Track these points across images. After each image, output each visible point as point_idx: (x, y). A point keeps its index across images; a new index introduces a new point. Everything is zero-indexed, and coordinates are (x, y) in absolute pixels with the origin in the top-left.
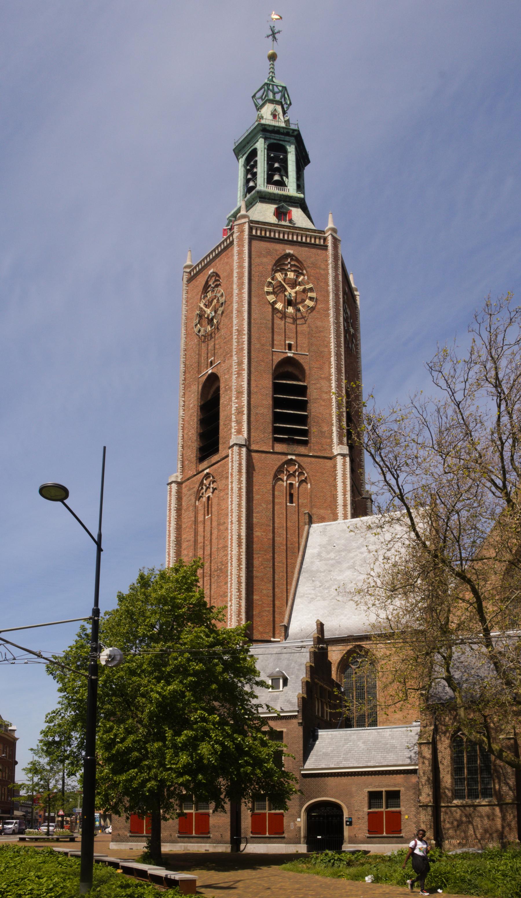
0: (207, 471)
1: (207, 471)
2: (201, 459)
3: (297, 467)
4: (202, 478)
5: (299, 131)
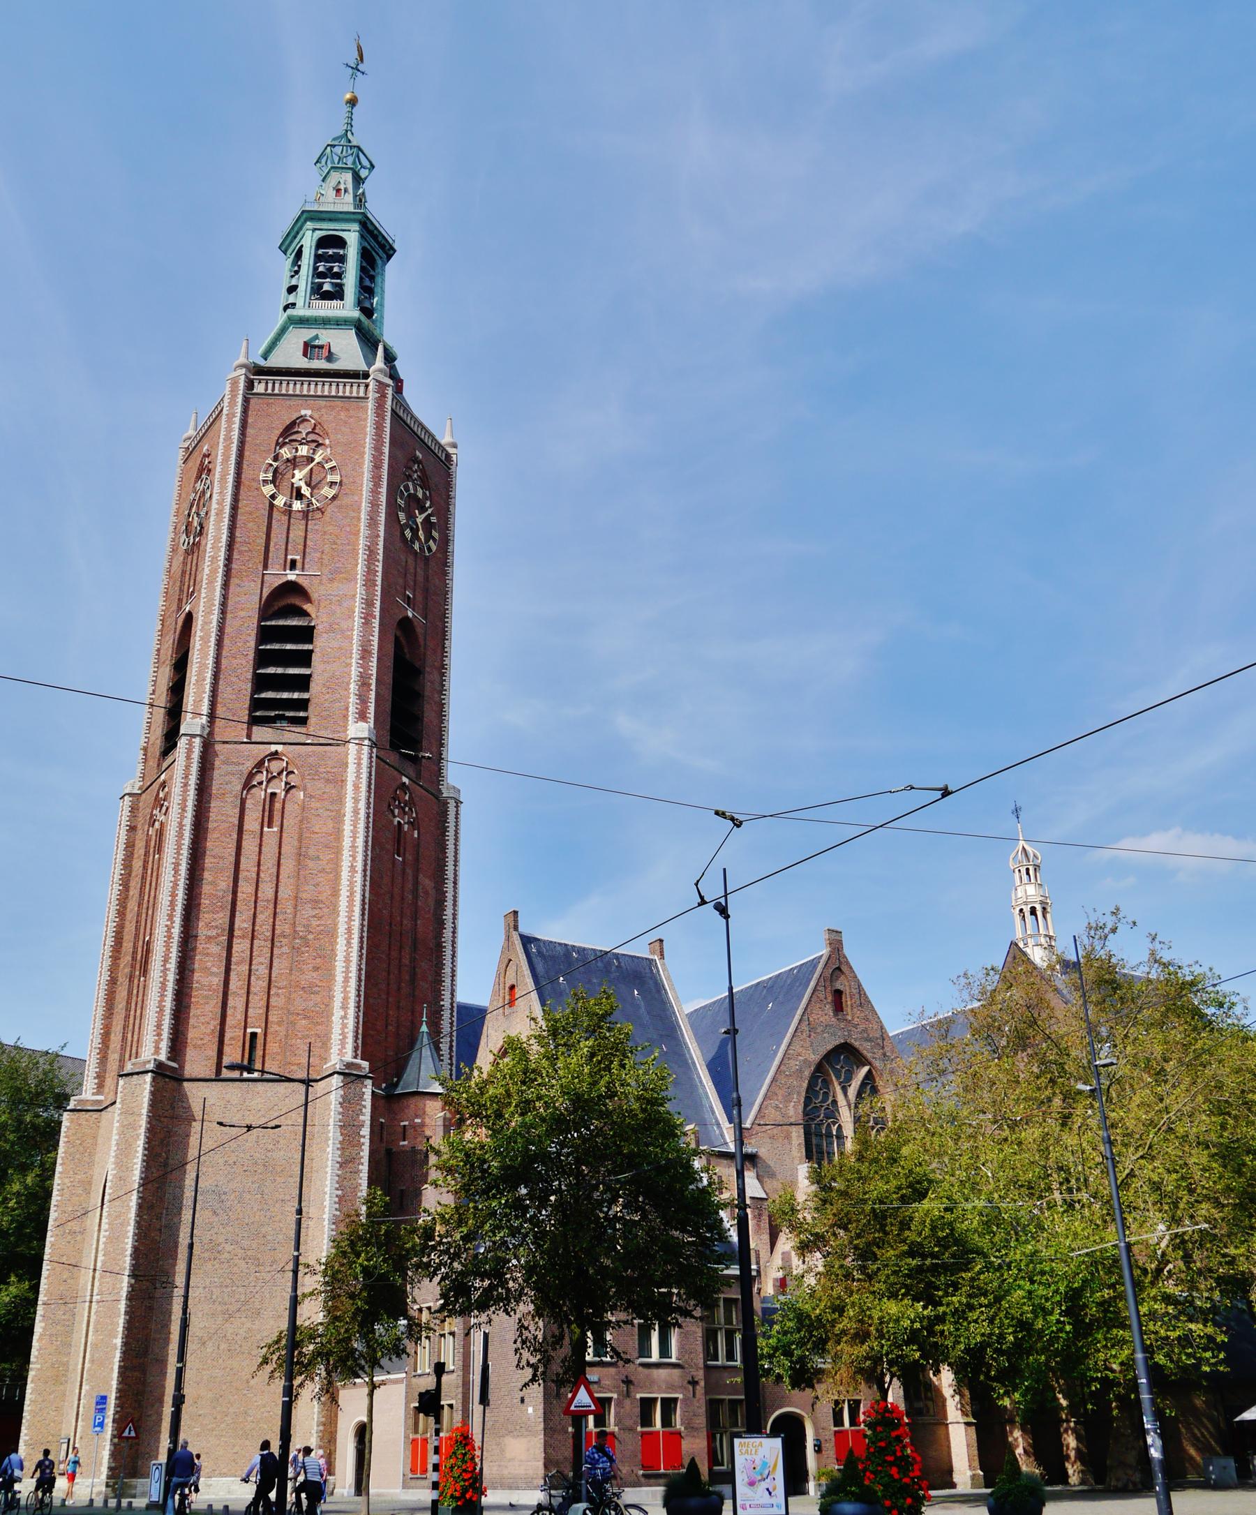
0: (280, 748)
1: (280, 748)
2: (254, 721)
3: (407, 798)
5: (395, 251)
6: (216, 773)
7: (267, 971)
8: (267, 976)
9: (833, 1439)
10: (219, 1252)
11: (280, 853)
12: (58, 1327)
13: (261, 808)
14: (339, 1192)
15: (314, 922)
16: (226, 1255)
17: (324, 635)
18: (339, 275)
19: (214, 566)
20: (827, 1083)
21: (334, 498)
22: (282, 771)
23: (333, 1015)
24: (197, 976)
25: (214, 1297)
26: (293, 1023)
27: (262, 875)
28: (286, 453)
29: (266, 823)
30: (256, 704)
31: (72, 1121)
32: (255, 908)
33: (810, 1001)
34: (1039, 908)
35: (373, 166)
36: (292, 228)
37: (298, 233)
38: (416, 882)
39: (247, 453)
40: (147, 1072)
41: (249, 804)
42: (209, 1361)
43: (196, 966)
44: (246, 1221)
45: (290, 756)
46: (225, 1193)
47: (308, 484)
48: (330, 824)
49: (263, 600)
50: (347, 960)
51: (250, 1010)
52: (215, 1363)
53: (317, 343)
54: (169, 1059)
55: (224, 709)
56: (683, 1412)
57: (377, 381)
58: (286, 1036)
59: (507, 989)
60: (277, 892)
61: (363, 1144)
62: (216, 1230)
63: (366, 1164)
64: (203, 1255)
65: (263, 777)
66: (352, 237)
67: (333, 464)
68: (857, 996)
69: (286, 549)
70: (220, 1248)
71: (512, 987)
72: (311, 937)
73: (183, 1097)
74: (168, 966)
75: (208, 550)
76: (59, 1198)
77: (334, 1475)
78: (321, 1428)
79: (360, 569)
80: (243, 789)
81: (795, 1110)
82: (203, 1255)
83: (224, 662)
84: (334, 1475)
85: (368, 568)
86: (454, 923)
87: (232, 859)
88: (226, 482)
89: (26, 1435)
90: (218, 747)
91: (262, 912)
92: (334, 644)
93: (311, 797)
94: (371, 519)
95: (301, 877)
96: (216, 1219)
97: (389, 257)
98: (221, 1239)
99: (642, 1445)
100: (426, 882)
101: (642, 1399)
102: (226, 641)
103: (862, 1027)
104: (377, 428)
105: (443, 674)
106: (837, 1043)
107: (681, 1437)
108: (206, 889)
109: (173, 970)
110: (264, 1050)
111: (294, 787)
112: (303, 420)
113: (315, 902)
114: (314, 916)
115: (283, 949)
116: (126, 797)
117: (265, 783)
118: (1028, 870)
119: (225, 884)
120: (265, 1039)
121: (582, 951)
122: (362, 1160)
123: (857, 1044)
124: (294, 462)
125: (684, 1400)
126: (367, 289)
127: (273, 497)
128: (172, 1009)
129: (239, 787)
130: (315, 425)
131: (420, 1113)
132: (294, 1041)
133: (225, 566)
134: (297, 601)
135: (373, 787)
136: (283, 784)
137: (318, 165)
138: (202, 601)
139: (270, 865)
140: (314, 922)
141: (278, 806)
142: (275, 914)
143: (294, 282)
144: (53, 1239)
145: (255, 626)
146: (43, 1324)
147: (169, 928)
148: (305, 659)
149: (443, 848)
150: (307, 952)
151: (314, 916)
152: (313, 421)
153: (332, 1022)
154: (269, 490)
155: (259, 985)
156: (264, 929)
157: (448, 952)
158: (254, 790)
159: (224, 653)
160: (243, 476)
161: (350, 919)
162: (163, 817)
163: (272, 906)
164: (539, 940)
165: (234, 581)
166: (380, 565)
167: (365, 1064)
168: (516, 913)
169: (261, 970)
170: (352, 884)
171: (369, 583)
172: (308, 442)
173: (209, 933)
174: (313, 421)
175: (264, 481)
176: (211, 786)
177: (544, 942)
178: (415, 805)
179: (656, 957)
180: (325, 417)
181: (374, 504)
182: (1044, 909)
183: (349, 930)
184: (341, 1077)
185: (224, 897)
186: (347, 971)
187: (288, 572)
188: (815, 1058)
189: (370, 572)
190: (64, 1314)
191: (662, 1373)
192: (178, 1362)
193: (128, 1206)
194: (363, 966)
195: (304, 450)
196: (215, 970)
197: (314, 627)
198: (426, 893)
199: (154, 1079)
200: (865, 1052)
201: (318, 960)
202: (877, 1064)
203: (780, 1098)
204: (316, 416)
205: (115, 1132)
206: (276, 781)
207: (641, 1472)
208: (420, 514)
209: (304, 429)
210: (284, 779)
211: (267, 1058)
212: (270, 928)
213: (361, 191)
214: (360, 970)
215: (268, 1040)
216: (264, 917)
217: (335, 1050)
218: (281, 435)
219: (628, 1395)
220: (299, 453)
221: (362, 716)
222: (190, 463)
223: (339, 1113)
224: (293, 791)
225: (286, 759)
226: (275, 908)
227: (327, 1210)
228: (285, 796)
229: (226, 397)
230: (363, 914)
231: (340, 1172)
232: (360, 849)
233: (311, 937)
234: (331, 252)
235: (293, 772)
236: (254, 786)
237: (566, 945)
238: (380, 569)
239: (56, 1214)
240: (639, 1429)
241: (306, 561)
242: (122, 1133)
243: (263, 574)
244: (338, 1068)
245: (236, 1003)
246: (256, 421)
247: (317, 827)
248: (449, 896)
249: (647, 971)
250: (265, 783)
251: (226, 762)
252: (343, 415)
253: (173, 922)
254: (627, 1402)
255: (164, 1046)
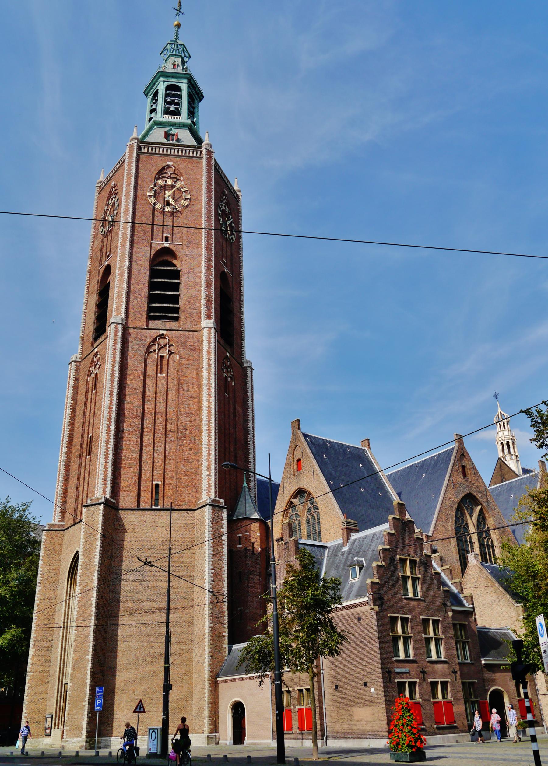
0: (165, 332)
1: (165, 332)
2: (150, 318)
3: (229, 364)
4: (155, 336)
6: (130, 345)
7: (163, 451)
8: (163, 453)
9: (518, 704)
10: (143, 606)
11: (167, 387)
12: (43, 652)
13: (156, 363)
14: (213, 571)
15: (189, 425)
16: (148, 607)
17: (186, 275)
18: (178, 104)
19: (125, 237)
20: (463, 514)
21: (187, 206)
22: (166, 344)
23: (202, 474)
24: (124, 452)
25: (142, 631)
26: (180, 479)
27: (158, 399)
28: (160, 182)
29: (159, 372)
30: (150, 309)
31: (47, 536)
32: (155, 416)
33: (452, 470)
34: (510, 441)
35: (190, 57)
36: (152, 81)
37: (155, 84)
38: (235, 409)
39: (139, 182)
40: (100, 504)
41: (149, 361)
42: (141, 668)
43: (124, 447)
44: (159, 588)
45: (170, 336)
46: (145, 573)
47: (173, 199)
48: (194, 373)
49: (152, 256)
50: (209, 444)
51: (155, 472)
52: (144, 669)
53: (171, 132)
54: (111, 497)
55: (133, 311)
56: (452, 689)
57: (207, 149)
58: (176, 486)
59: (295, 461)
60: (166, 408)
61: (224, 544)
62: (141, 593)
63: (226, 556)
64: (134, 608)
65: (156, 347)
66: (184, 86)
67: (186, 189)
68: (472, 469)
69: (163, 231)
70: (144, 604)
71: (299, 460)
72: (187, 432)
73: (119, 519)
74: (109, 446)
75: (121, 230)
76: (41, 579)
77: (218, 732)
78: (210, 705)
79: (204, 241)
80: (146, 353)
81: (451, 527)
82: (134, 608)
83: (132, 287)
84: (218, 732)
85: (208, 241)
86: (253, 431)
87: (141, 390)
88: (129, 196)
89: (26, 713)
90: (131, 331)
91: (159, 419)
92: (191, 279)
93: (183, 358)
94: (208, 217)
95: (180, 400)
96: (141, 587)
97: (201, 100)
98: (144, 598)
99: (434, 710)
100: (239, 409)
101: (431, 682)
102: (133, 276)
103: (476, 485)
104: (208, 172)
105: (241, 304)
106: (466, 493)
107: (453, 705)
108: (127, 406)
109: (111, 448)
110: (164, 493)
111: (173, 353)
112: (169, 167)
113: (188, 414)
114: (188, 421)
115: (171, 438)
116: (73, 363)
117: (157, 350)
118: (504, 423)
119: (137, 403)
120: (164, 488)
121: (331, 443)
122: (224, 553)
123: (475, 494)
124: (164, 188)
125: (452, 682)
126: (192, 113)
127: (155, 204)
128: (112, 470)
129: (143, 352)
130: (175, 170)
131: (248, 529)
132: (180, 489)
133: (131, 237)
134: (169, 259)
135: (217, 353)
136: (167, 351)
137: (162, 54)
138: (118, 255)
139: (162, 394)
140: (189, 425)
141: (165, 362)
142: (166, 420)
143: (154, 107)
144: (38, 602)
145: (148, 268)
146: (34, 650)
147: (109, 426)
148: (176, 287)
149: (245, 392)
150: (185, 440)
151: (188, 421)
152: (174, 168)
153: (202, 478)
154: (152, 200)
155: (159, 458)
156: (160, 428)
157: (251, 447)
158: (151, 354)
159: (132, 282)
160: (138, 193)
161: (209, 422)
162: (97, 371)
163: (164, 416)
164: (310, 436)
165: (135, 246)
166: (213, 240)
167: (222, 501)
168: (298, 420)
169: (160, 450)
170: (209, 403)
171: (208, 249)
172: (172, 178)
173: (130, 430)
174: (174, 168)
175: (149, 196)
176: (128, 351)
177: (313, 437)
178: (232, 368)
179: (366, 448)
180: (180, 166)
181: (209, 210)
182: (513, 442)
183: (209, 428)
184: (211, 507)
185: (137, 410)
186: (209, 450)
187: (164, 242)
188: (457, 500)
189: (208, 244)
190: (46, 644)
191: (439, 667)
192: (165, 664)
193: (92, 579)
194: (217, 448)
195: (170, 182)
196: (134, 449)
197: (179, 271)
198: (239, 415)
199: (104, 508)
200: (479, 498)
201: (192, 445)
202: (485, 504)
203: (444, 520)
204: (175, 165)
205: (82, 537)
206: (163, 349)
207: (436, 726)
208: (228, 220)
209: (169, 172)
210: (168, 349)
211: (165, 498)
212: (164, 428)
213: (185, 66)
214: (216, 450)
215: (166, 488)
216: (160, 421)
217: (204, 493)
218: (157, 174)
219: (424, 680)
220: (168, 183)
221: (209, 317)
222: (103, 193)
223: (211, 527)
224: (173, 355)
225: (168, 338)
226: (166, 416)
227: (207, 581)
228: (169, 357)
229: (127, 154)
230: (216, 420)
231: (213, 560)
232: (213, 385)
233: (187, 432)
234: (173, 92)
235: (172, 345)
236: (151, 352)
237: (323, 439)
238: (213, 243)
239: (40, 588)
240: (432, 700)
241: (174, 237)
242: (86, 538)
243: (151, 243)
244: (208, 502)
245: (147, 468)
246: (143, 166)
247: (187, 374)
248: (250, 417)
249: (363, 455)
250: (157, 350)
251: (136, 339)
252: (189, 165)
253: (110, 423)
254: (424, 684)
255: (108, 490)
